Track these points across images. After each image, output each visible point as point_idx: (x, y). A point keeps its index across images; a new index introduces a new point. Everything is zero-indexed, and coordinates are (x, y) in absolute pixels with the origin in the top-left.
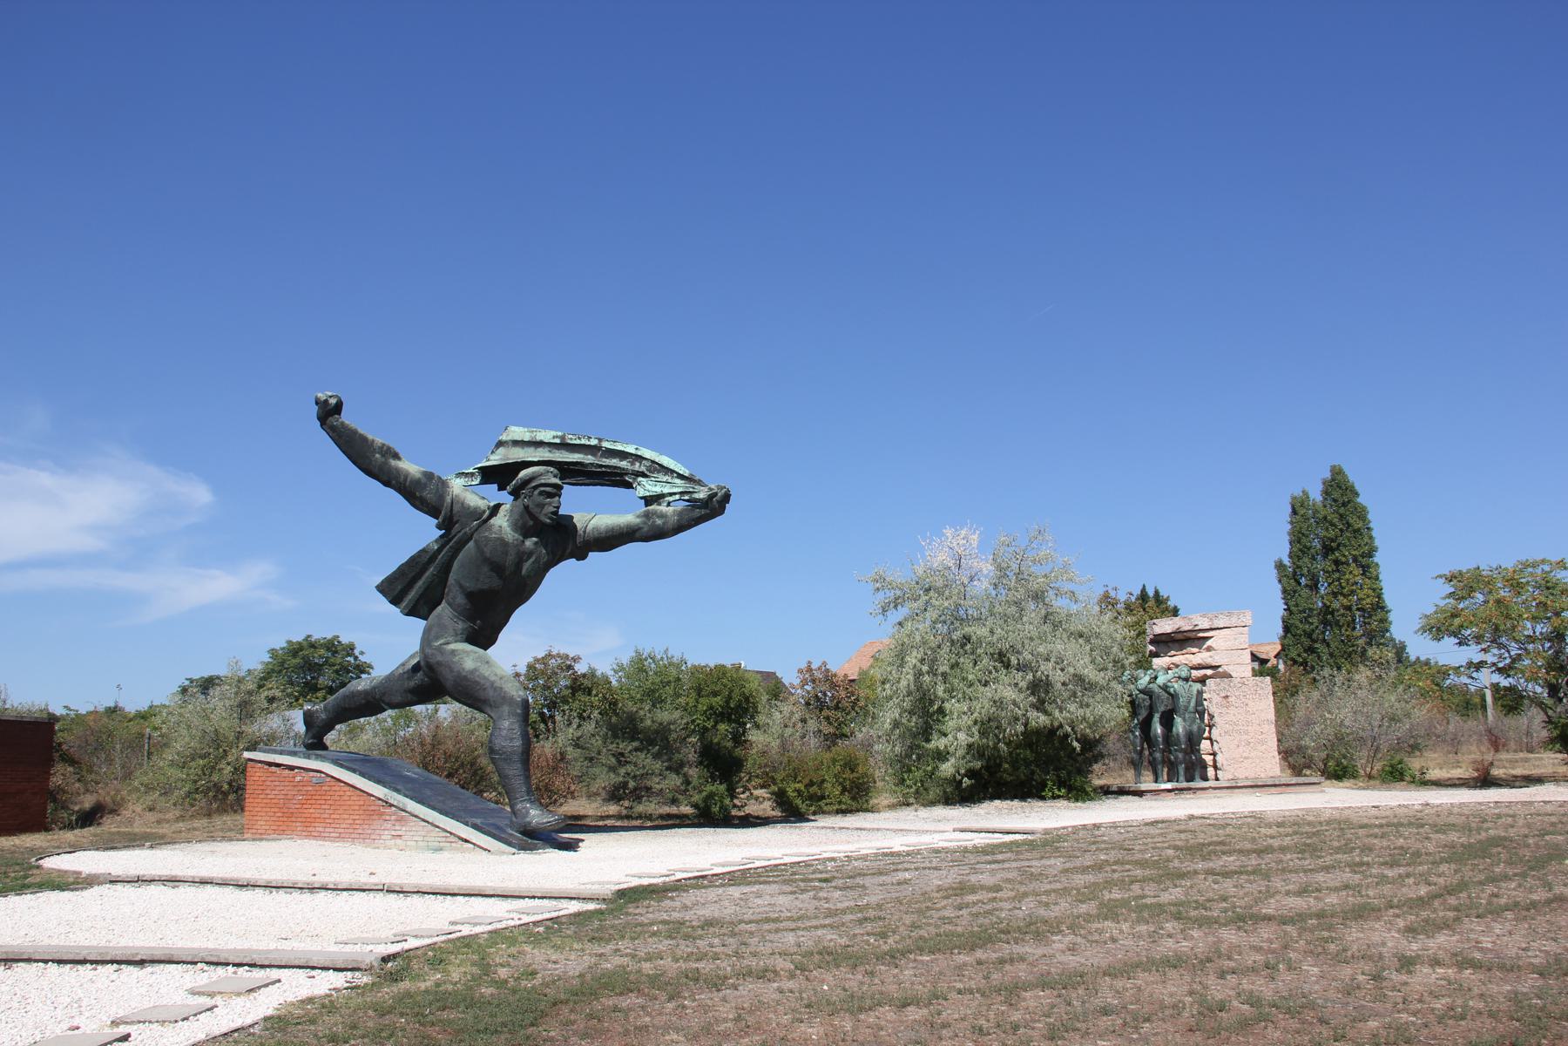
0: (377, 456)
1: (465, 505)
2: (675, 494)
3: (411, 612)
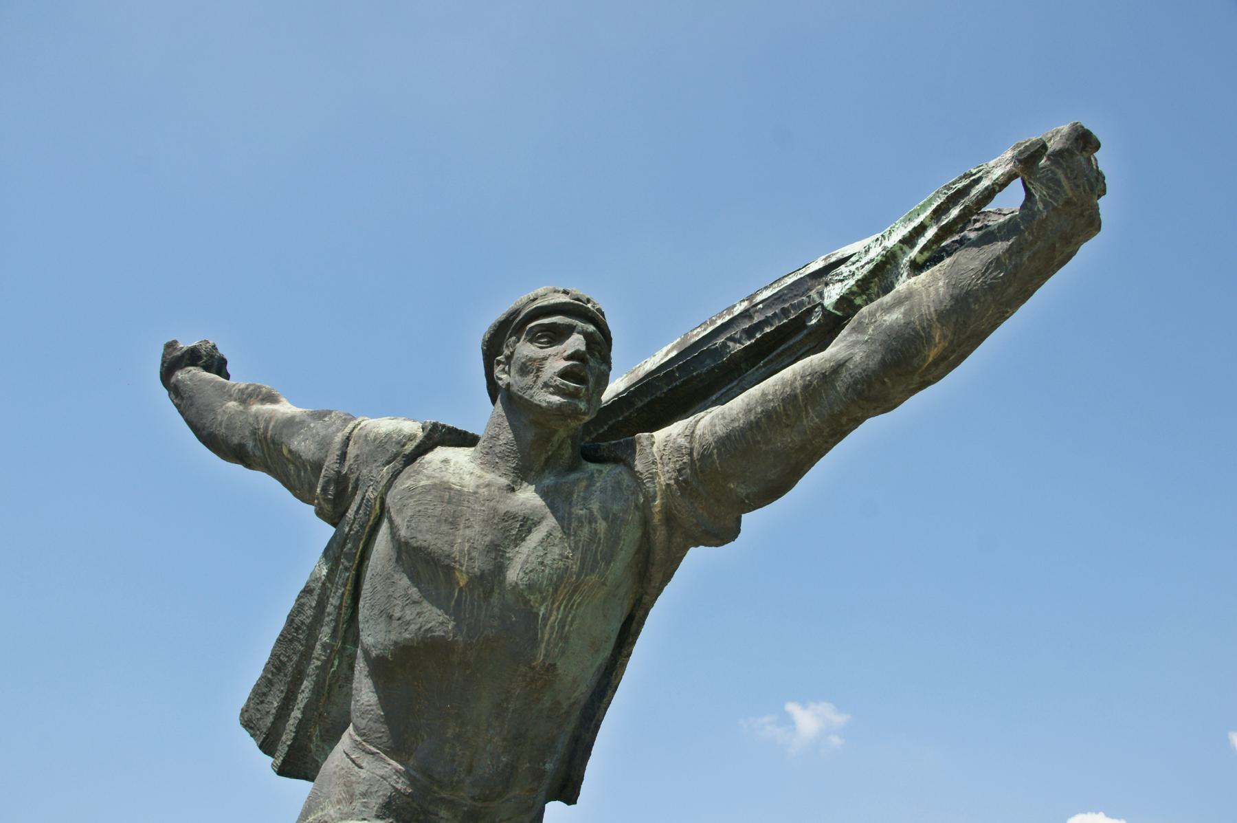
2: (920, 230)
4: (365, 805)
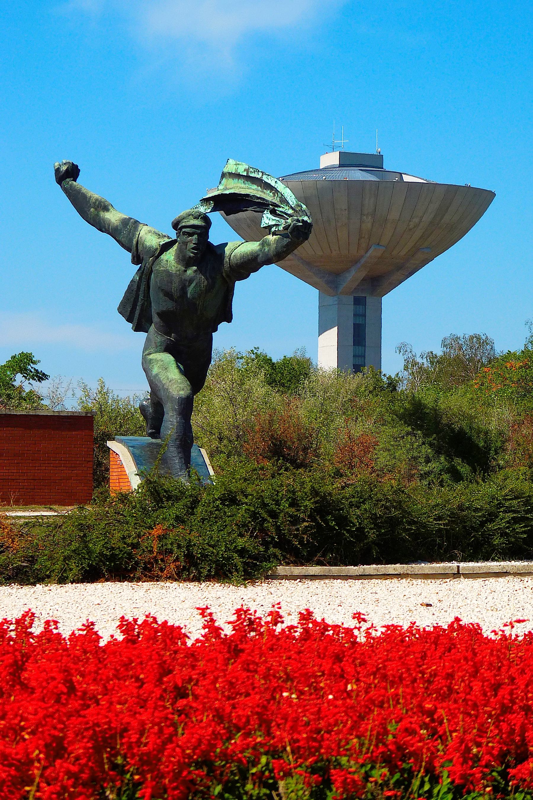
0: (92, 210)
1: (145, 246)
3: (138, 328)
4: (161, 348)
